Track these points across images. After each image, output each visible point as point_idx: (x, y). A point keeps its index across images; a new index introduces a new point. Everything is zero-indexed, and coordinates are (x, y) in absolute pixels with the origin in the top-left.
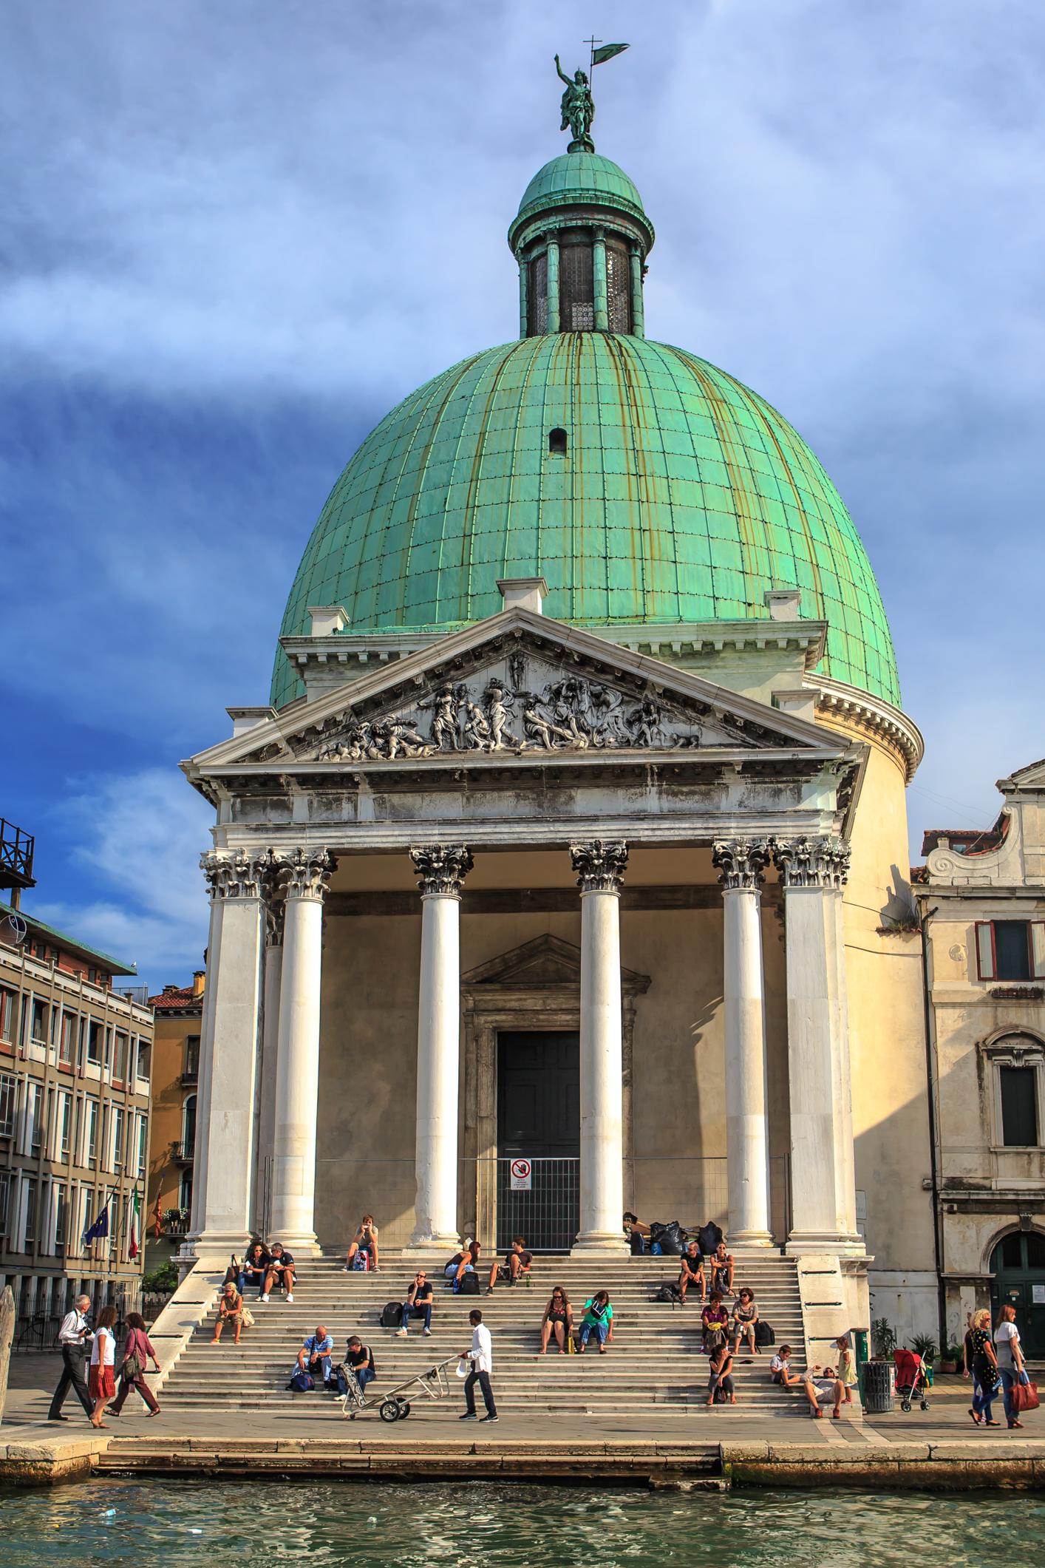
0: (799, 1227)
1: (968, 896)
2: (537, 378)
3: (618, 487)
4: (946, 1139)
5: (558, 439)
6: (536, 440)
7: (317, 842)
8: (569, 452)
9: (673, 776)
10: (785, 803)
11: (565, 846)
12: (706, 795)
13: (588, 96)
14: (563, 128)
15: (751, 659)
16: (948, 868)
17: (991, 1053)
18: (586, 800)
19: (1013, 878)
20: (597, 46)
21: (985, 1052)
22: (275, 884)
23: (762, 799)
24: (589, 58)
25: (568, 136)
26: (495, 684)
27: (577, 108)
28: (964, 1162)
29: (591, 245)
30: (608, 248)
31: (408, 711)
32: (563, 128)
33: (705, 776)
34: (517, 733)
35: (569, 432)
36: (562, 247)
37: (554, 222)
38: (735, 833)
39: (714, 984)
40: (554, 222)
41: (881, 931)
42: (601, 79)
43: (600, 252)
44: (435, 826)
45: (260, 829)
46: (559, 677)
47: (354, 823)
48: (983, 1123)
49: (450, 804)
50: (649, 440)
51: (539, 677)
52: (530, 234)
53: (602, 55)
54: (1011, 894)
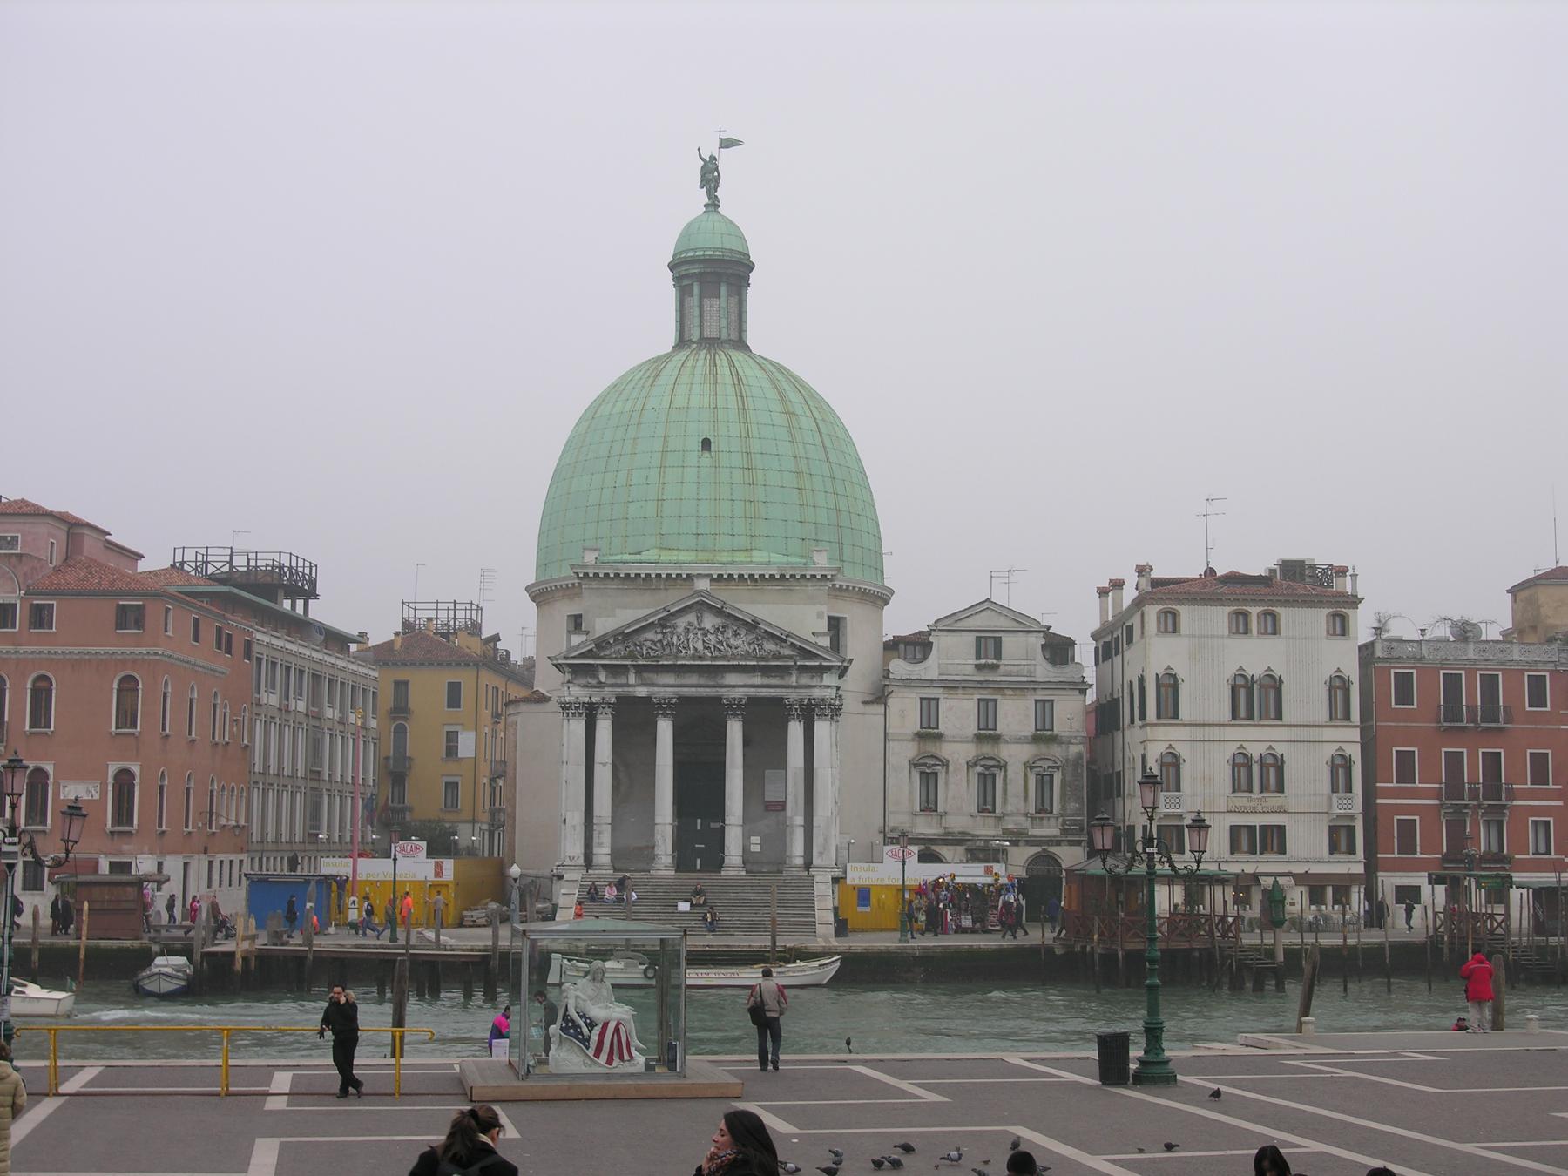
0: (815, 862)
1: (909, 683)
2: (695, 401)
3: (738, 476)
4: (891, 807)
5: (706, 444)
7: (610, 694)
9: (766, 670)
10: (815, 682)
11: (719, 698)
12: (782, 678)
15: (803, 582)
16: (899, 668)
17: (915, 765)
18: (731, 679)
19: (933, 675)
21: (914, 764)
22: (590, 713)
23: (805, 680)
24: (718, 143)
26: (690, 624)
27: (710, 177)
28: (899, 820)
30: (728, 284)
31: (650, 635)
33: (783, 671)
34: (700, 646)
36: (701, 284)
37: (695, 269)
38: (792, 696)
39: (781, 762)
41: (865, 703)
42: (726, 160)
43: (723, 290)
44: (666, 688)
45: (585, 686)
46: (718, 621)
47: (628, 685)
48: (911, 801)
49: (669, 679)
50: (756, 446)
51: (710, 622)
52: (683, 270)
53: (727, 143)
54: (930, 684)
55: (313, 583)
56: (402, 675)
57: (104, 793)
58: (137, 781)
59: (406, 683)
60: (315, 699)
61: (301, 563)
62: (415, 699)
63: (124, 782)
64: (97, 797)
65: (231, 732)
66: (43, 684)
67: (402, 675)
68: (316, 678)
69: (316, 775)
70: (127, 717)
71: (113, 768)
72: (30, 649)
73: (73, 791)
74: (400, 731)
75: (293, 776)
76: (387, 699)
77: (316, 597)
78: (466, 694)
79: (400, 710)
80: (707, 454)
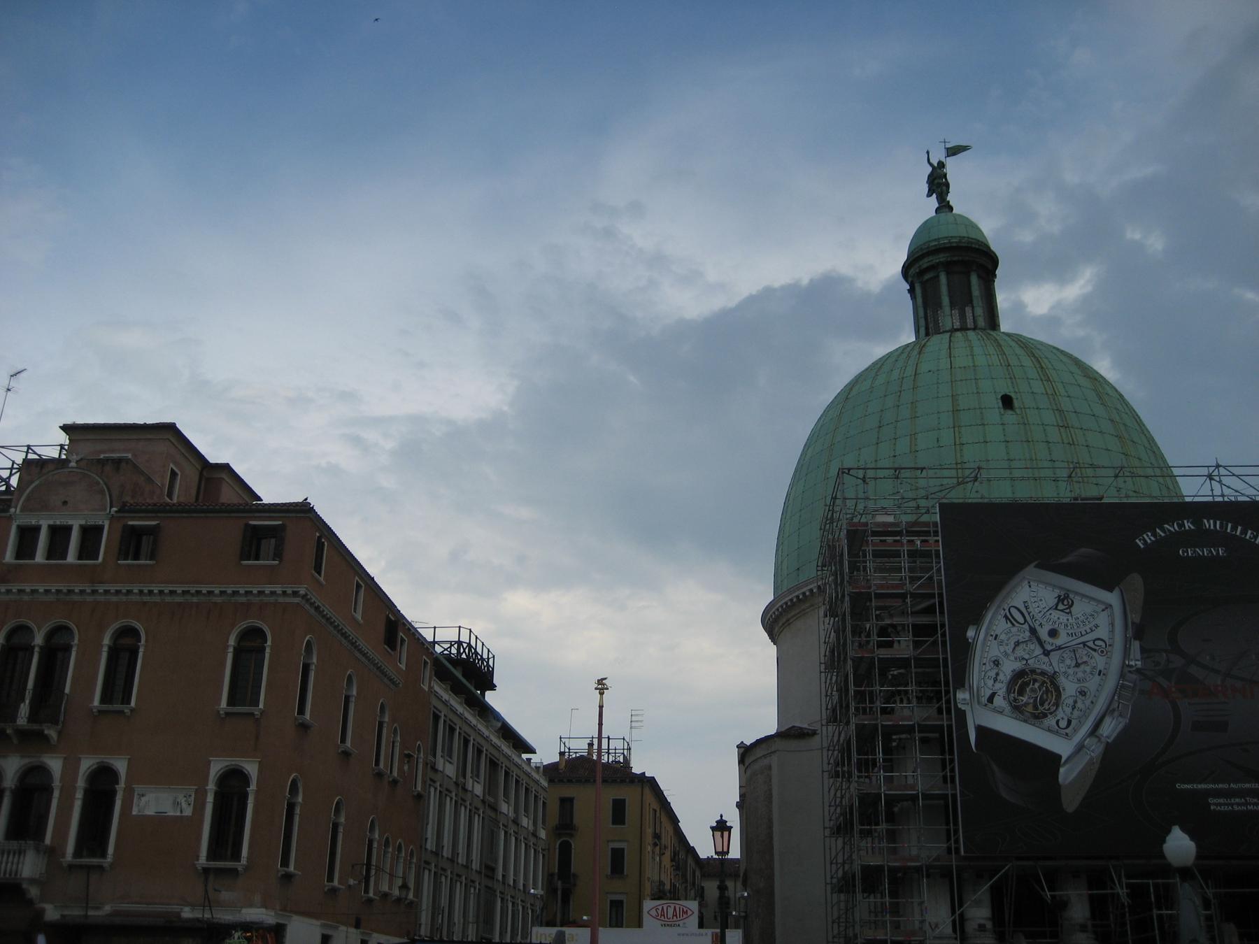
5: (1007, 402)
6: (995, 403)
8: (1018, 411)
13: (945, 175)
14: (929, 195)
20: (948, 146)
25: (933, 202)
27: (938, 184)
29: (968, 274)
32: (929, 195)
35: (1013, 395)
36: (948, 274)
37: (942, 258)
40: (942, 258)
43: (974, 279)
52: (925, 263)
53: (953, 151)
55: (491, 674)
56: (567, 791)
57: (199, 807)
58: (253, 787)
59: (571, 800)
60: (491, 787)
61: (479, 645)
62: (582, 817)
63: (233, 782)
64: (188, 812)
65: (400, 769)
66: (127, 641)
67: (567, 791)
68: (493, 764)
69: (489, 870)
70: (243, 689)
71: (216, 767)
72: (113, 588)
73: (155, 802)
74: (565, 850)
75: (467, 867)
76: (554, 820)
77: (492, 687)
78: (631, 812)
79: (565, 827)
80: (1010, 412)
